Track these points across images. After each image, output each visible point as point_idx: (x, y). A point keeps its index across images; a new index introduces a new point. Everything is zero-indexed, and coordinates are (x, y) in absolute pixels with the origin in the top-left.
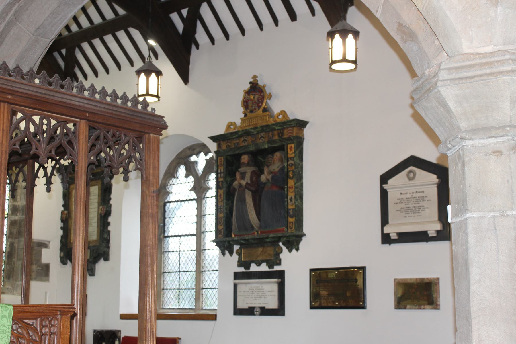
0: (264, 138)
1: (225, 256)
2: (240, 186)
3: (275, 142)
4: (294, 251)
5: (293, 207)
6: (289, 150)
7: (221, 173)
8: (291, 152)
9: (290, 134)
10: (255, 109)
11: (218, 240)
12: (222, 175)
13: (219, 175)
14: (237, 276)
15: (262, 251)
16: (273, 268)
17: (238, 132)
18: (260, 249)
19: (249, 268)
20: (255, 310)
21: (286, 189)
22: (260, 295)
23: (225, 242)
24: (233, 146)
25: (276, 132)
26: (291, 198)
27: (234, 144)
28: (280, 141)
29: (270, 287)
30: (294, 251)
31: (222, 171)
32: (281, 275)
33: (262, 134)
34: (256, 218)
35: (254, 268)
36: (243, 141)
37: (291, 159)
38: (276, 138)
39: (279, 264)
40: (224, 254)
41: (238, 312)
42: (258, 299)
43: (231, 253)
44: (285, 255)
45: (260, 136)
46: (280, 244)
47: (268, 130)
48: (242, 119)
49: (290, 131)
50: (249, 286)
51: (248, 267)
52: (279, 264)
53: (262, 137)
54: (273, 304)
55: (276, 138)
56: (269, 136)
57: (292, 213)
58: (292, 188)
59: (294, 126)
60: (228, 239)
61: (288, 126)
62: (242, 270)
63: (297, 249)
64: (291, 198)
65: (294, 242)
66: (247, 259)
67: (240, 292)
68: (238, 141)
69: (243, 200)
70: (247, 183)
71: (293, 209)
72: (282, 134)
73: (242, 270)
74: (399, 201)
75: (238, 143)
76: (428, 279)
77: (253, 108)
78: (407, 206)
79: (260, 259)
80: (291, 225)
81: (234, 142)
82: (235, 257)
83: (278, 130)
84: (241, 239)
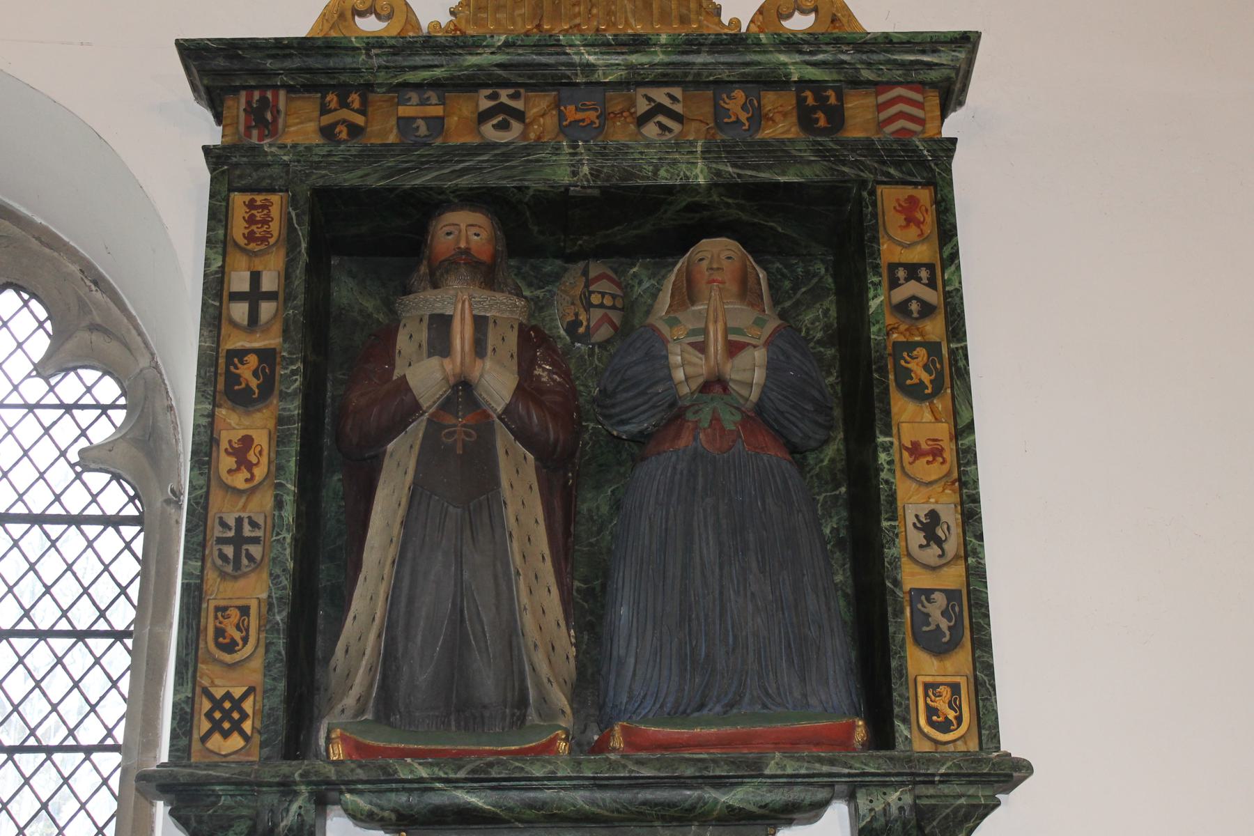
3: (777, 153)
7: (254, 296)
8: (913, 232)
9: (901, 123)
11: (183, 773)
17: (473, 45)
24: (392, 138)
26: (934, 516)
27: (405, 124)
28: (822, 152)
33: (660, 95)
36: (484, 117)
38: (782, 128)
53: (659, 109)
55: (782, 128)
56: (719, 112)
60: (295, 770)
61: (897, 74)
64: (934, 516)
68: (438, 111)
71: (952, 595)
72: (837, 117)
75: (437, 124)
80: (941, 704)
81: (403, 111)
83: (803, 83)
84: (478, 780)
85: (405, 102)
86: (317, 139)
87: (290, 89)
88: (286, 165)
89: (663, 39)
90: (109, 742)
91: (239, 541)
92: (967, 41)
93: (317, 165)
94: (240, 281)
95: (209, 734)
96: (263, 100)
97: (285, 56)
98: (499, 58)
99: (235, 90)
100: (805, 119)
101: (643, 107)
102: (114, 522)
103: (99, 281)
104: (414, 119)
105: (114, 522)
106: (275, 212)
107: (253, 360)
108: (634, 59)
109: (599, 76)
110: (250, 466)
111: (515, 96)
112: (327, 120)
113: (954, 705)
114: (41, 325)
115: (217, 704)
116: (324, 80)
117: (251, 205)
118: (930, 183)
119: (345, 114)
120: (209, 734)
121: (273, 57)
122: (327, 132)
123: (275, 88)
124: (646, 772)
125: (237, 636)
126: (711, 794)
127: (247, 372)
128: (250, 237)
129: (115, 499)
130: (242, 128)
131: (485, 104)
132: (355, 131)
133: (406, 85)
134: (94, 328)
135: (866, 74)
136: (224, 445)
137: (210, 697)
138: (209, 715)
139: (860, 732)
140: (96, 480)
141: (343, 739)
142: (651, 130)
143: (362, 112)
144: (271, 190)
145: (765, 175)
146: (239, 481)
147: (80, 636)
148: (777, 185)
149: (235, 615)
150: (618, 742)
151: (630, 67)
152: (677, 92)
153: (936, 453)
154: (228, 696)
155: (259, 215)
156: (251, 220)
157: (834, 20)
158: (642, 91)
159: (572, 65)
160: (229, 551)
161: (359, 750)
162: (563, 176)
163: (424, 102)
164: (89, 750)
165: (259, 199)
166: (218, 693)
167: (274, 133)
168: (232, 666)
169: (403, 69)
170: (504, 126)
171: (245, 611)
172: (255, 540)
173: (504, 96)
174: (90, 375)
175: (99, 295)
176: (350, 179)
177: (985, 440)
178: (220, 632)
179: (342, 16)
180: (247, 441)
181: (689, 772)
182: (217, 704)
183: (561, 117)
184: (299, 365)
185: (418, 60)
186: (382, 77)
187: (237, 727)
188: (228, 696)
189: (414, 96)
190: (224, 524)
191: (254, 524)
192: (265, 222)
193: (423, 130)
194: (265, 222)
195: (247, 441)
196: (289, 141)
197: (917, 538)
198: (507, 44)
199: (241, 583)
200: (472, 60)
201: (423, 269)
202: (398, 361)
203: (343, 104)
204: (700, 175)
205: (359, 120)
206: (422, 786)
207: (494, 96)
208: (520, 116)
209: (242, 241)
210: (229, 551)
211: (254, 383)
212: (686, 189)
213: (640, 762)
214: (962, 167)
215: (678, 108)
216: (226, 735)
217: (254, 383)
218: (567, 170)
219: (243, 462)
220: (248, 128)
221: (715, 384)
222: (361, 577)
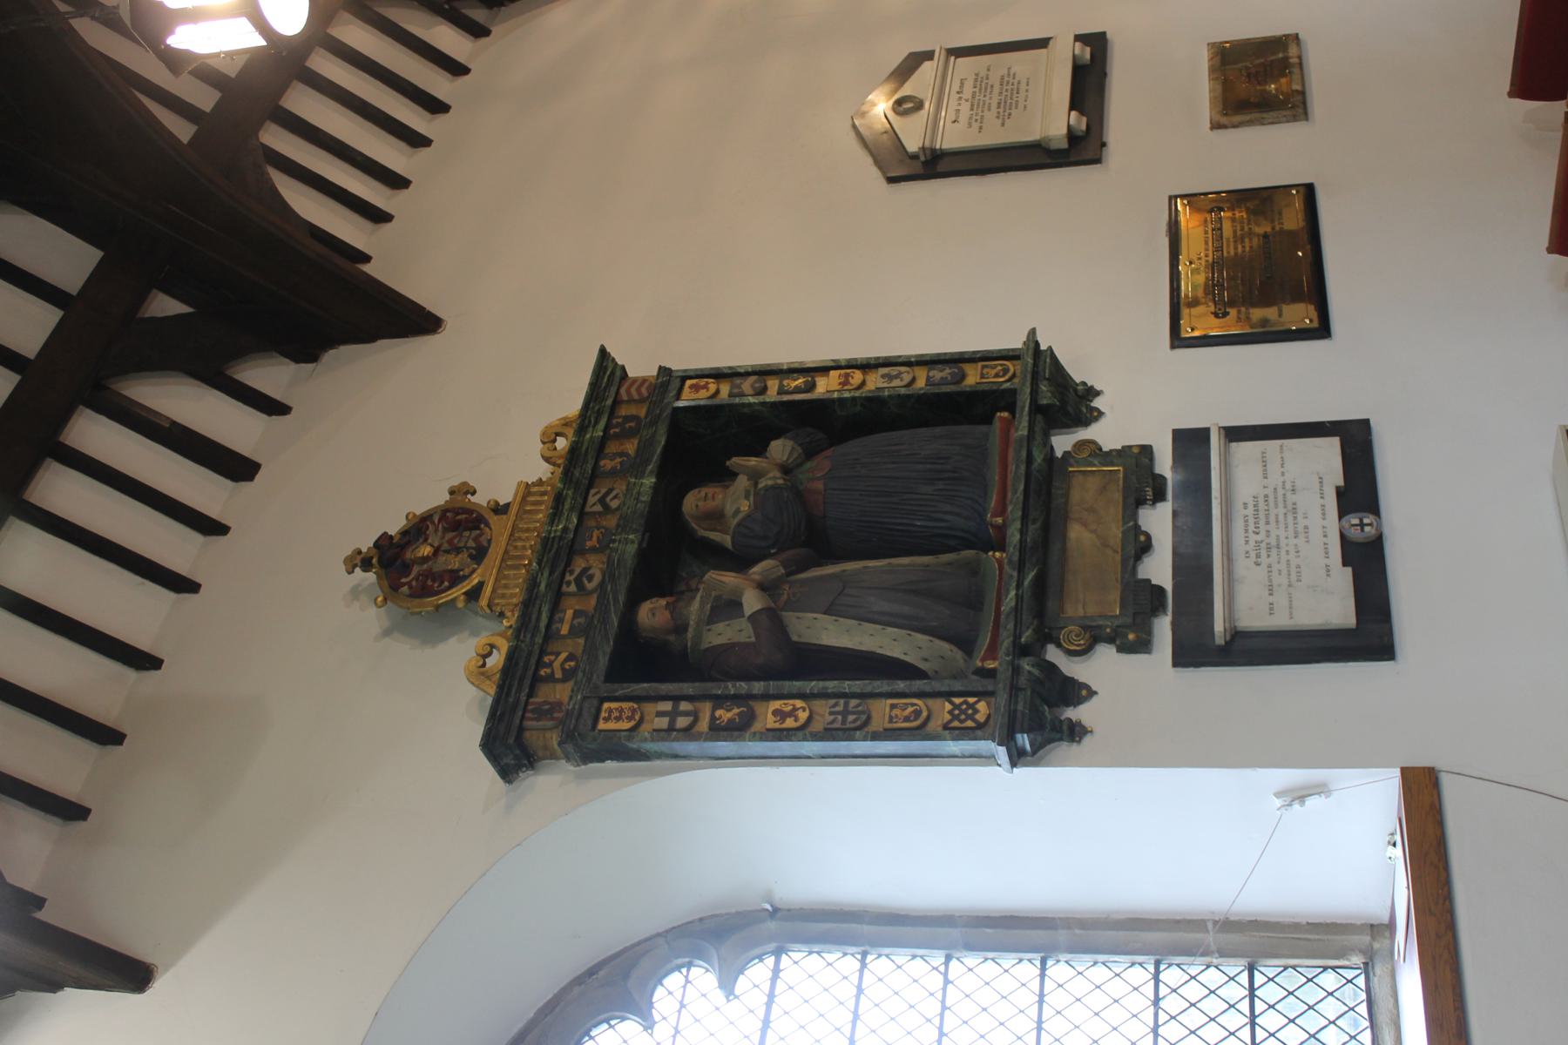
0: (611, 490)
1: (1086, 722)
4: (1097, 403)
10: (476, 539)
12: (685, 706)
14: (1194, 651)
15: (1085, 525)
18: (1076, 532)
19: (1160, 591)
20: (1354, 534)
22: (1281, 510)
24: (581, 641)
29: (1245, 475)
30: (1097, 403)
31: (667, 706)
32: (1191, 443)
33: (592, 499)
35: (1159, 569)
37: (739, 387)
39: (1147, 451)
40: (1075, 732)
42: (1302, 522)
43: (1075, 692)
44: (1108, 433)
47: (589, 467)
50: (1243, 566)
52: (1147, 451)
53: (602, 501)
56: (613, 473)
62: (1163, 628)
63: (1092, 393)
66: (1115, 596)
68: (570, 613)
74: (976, 126)
75: (577, 614)
76: (1211, 59)
77: (471, 544)
78: (994, 105)
81: (565, 630)
82: (1102, 669)
85: (559, 630)
86: (570, 685)
87: (530, 695)
88: (584, 698)
89: (560, 485)
90: (942, 968)
91: (845, 713)
92: (603, 353)
93: (589, 680)
94: (663, 722)
95: (974, 720)
96: (532, 711)
97: (510, 689)
98: (546, 574)
99: (521, 729)
100: (626, 435)
101: (599, 508)
102: (776, 971)
103: (591, 972)
104: (572, 627)
105: (776, 971)
106: (613, 705)
107: (718, 713)
108: (567, 506)
109: (572, 527)
110: (795, 709)
111: (572, 572)
112: (558, 675)
113: (994, 367)
114: (611, 1027)
115: (955, 718)
116: (530, 673)
117: (606, 720)
118: (684, 379)
119: (557, 665)
120: (974, 720)
121: (508, 695)
122: (568, 675)
123: (527, 704)
124: (1022, 487)
125: (910, 709)
126: (1035, 466)
127: (725, 715)
128: (630, 719)
129: (759, 972)
130: (550, 724)
131: (573, 588)
132: (571, 657)
133: (548, 626)
134: (626, 976)
135: (609, 402)
136: (777, 725)
137: (950, 721)
138: (962, 722)
139: (1005, 414)
140: (742, 983)
141: (983, 660)
142: (614, 504)
143: (558, 654)
144: (599, 711)
145: (659, 450)
146: (803, 716)
147: (860, 990)
148: (665, 447)
149: (895, 712)
150: (1000, 520)
151: (572, 509)
152: (593, 491)
153: (847, 375)
154: (950, 712)
155: (616, 714)
156: (618, 719)
157: (566, 425)
158: (588, 509)
159: (561, 538)
160: (851, 718)
161: (992, 652)
162: (632, 549)
163: (562, 621)
164: (944, 1008)
165: (603, 714)
166: (948, 717)
167: (560, 704)
168: (928, 718)
169: (537, 627)
170: (590, 578)
171: (893, 706)
172: (846, 704)
173: (568, 577)
174: (659, 992)
175: (602, 973)
176: (603, 661)
177: (843, 355)
178: (907, 719)
179: (483, 674)
180: (775, 713)
181: (1023, 467)
182: (955, 718)
183: (593, 550)
184: (730, 685)
185: (534, 617)
186: (539, 640)
187: (971, 706)
188: (950, 712)
189: (554, 627)
190: (833, 722)
191: (836, 705)
192: (621, 711)
193: (581, 620)
194: (621, 711)
195: (775, 713)
196: (566, 700)
197: (896, 383)
198: (539, 563)
199: (874, 715)
200: (543, 587)
201: (672, 638)
202: (736, 640)
203: (550, 664)
204: (649, 481)
205: (563, 656)
206: (1019, 598)
207: (569, 583)
208: (585, 570)
209: (632, 723)
210: (851, 718)
211: (736, 711)
212: (656, 488)
213: (1015, 492)
214: (677, 365)
215: (603, 491)
216: (976, 711)
217: (736, 711)
218: (629, 547)
219: (793, 713)
220: (553, 719)
221: (786, 470)
222: (880, 651)
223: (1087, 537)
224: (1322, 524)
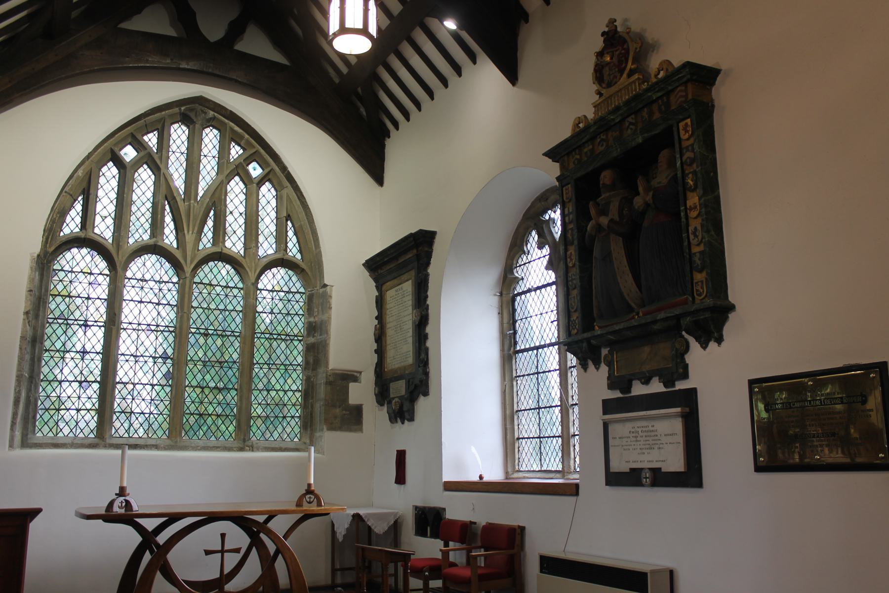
2: (599, 228)
5: (702, 248)
6: (682, 132)
13: (567, 219)
16: (673, 385)
19: (630, 392)
21: (682, 214)
23: (581, 341)
25: (655, 107)
33: (630, 119)
34: (634, 288)
41: (614, 479)
43: (597, 365)
45: (627, 124)
46: (684, 333)
48: (596, 106)
49: (681, 94)
50: (629, 426)
51: (627, 389)
53: (631, 123)
54: (675, 462)
57: (699, 262)
58: (695, 207)
59: (686, 83)
62: (617, 394)
65: (711, 323)
67: (614, 438)
69: (607, 257)
70: (611, 221)
73: (617, 394)
79: (646, 368)
161: (600, 327)
223: (646, 355)
224: (646, 460)
